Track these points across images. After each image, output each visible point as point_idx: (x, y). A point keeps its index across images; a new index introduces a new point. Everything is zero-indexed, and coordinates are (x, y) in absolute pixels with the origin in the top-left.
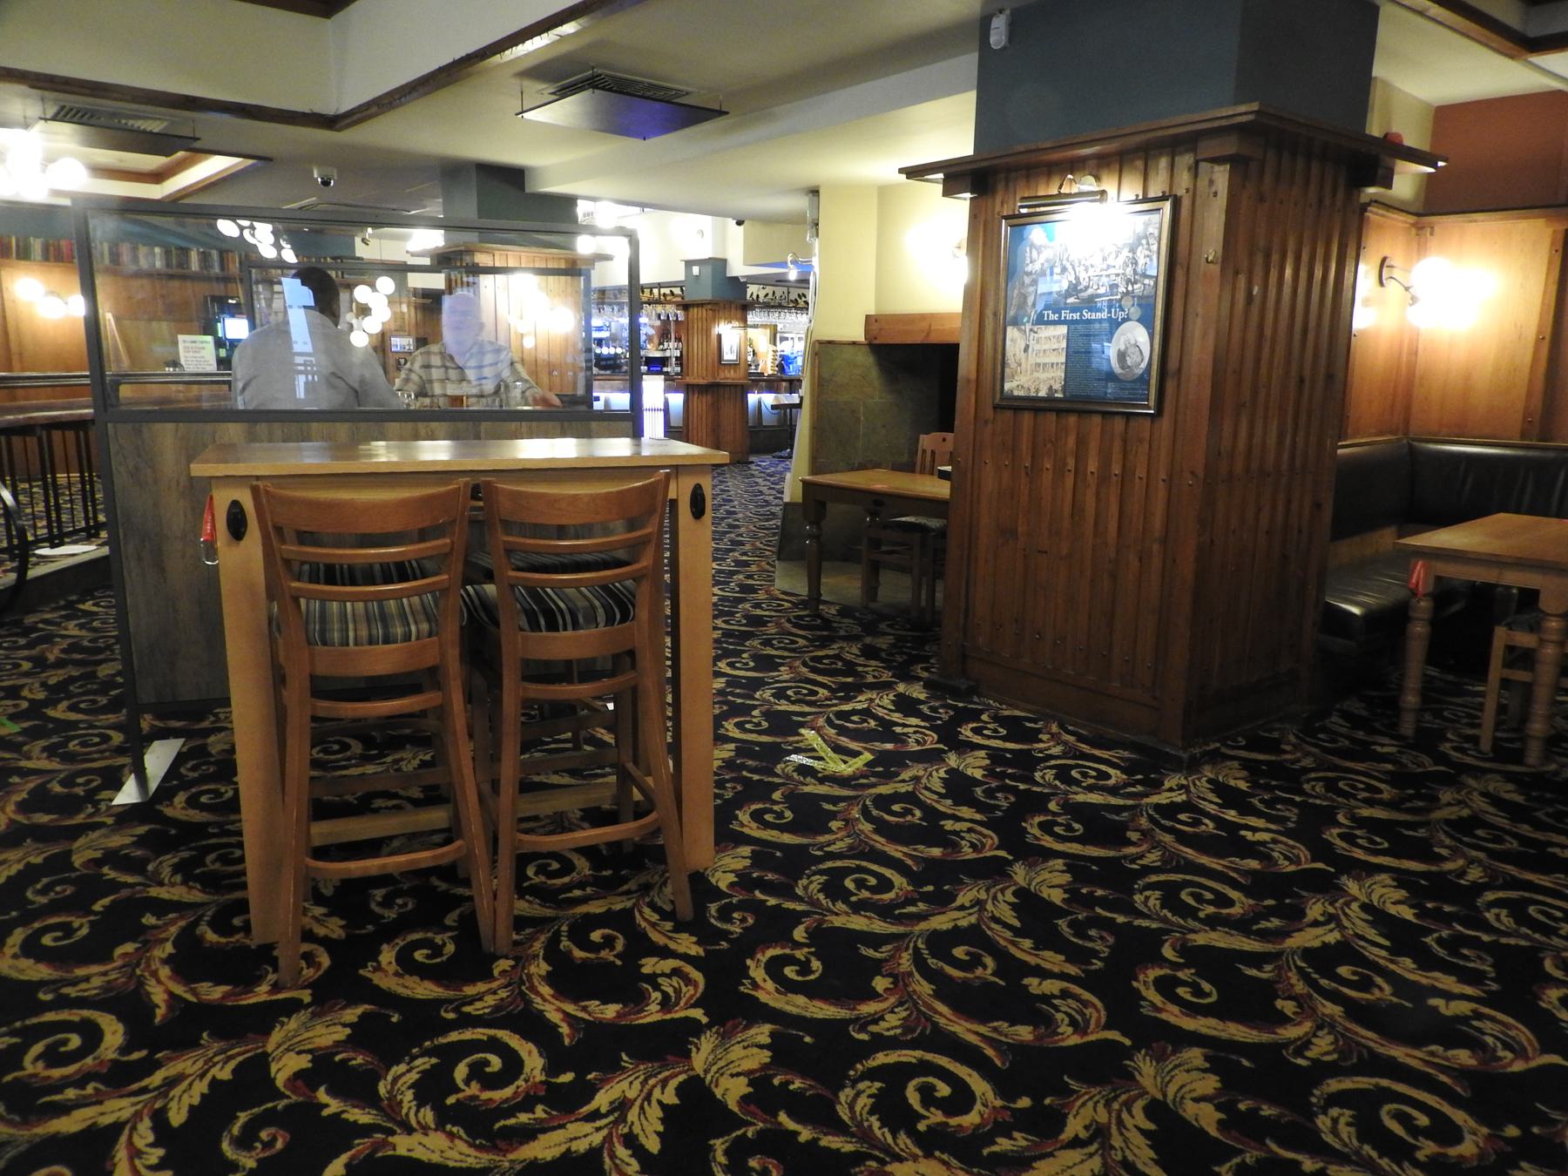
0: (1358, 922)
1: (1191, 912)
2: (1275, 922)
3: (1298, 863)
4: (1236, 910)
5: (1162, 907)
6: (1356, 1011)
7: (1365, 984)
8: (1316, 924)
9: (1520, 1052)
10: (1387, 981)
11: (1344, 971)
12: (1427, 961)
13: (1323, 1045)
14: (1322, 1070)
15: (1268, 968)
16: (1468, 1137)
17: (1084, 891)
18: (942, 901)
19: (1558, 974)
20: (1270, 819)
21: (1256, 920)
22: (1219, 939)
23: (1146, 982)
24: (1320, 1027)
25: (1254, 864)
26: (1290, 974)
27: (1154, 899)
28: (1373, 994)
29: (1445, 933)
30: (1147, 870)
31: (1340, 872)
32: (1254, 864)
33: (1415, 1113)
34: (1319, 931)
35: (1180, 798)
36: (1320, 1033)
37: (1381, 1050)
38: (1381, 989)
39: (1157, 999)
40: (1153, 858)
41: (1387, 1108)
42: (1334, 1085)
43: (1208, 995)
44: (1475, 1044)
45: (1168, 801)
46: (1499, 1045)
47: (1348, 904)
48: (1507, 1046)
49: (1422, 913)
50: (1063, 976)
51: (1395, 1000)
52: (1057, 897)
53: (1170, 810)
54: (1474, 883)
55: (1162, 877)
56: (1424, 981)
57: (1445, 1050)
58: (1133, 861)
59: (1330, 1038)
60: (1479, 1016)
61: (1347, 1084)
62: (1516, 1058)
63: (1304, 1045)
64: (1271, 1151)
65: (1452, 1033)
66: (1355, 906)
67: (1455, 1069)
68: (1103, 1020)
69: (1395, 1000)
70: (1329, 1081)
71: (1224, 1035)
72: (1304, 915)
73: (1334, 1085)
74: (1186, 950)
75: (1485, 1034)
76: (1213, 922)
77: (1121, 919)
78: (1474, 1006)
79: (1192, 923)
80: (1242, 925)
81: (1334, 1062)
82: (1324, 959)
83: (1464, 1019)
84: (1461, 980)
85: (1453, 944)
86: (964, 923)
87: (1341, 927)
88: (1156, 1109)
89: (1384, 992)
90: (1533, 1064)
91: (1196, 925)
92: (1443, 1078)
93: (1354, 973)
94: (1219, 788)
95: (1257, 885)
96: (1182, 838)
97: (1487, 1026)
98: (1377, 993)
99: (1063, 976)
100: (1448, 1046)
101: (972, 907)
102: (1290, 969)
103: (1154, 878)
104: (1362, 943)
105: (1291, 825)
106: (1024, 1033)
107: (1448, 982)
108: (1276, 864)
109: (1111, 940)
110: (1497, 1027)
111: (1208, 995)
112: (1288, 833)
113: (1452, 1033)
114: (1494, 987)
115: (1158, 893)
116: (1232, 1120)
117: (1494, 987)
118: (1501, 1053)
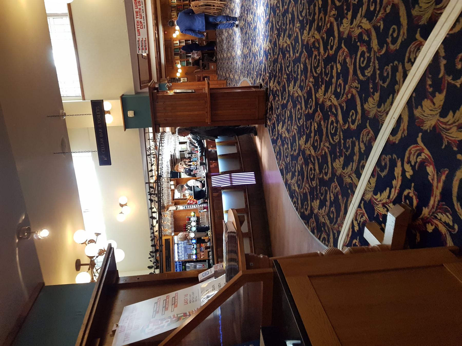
0: (308, 145)
1: (314, 175)
2: (312, 159)
3: (302, 158)
4: (312, 166)
5: (314, 180)
6: (321, 141)
9: (319, 114)
10: (315, 137)
11: (316, 144)
12: (311, 132)
13: (327, 144)
14: (330, 144)
16: (332, 119)
17: (316, 197)
18: (324, 224)
19: (307, 111)
20: (295, 166)
21: (312, 162)
22: (317, 168)
23: (326, 178)
25: (304, 166)
27: (313, 182)
29: (306, 130)
30: (310, 186)
31: (301, 150)
32: (304, 166)
33: (331, 128)
34: (311, 151)
35: (296, 185)
39: (328, 175)
40: (307, 186)
41: (332, 132)
42: (332, 141)
43: (325, 166)
45: (297, 187)
47: (306, 147)
49: (304, 134)
50: (330, 194)
52: (318, 201)
53: (299, 186)
54: (297, 127)
55: (310, 182)
56: (313, 131)
58: (309, 189)
61: (331, 139)
63: (328, 148)
64: (343, 148)
66: (306, 146)
68: (334, 183)
71: (330, 161)
72: (310, 154)
73: (332, 141)
74: (320, 173)
76: (315, 170)
77: (318, 187)
79: (316, 174)
80: (314, 164)
82: (315, 148)
84: (312, 125)
85: (307, 128)
86: (327, 218)
87: (310, 148)
88: (343, 169)
90: (320, 112)
91: (316, 172)
94: (292, 178)
95: (307, 164)
96: (303, 182)
98: (317, 138)
99: (330, 194)
101: (324, 218)
103: (310, 184)
105: (296, 162)
106: (340, 197)
108: (302, 162)
109: (322, 187)
111: (325, 166)
112: (297, 162)
114: (311, 120)
115: (313, 182)
116: (341, 155)
117: (311, 120)
118: (320, 117)
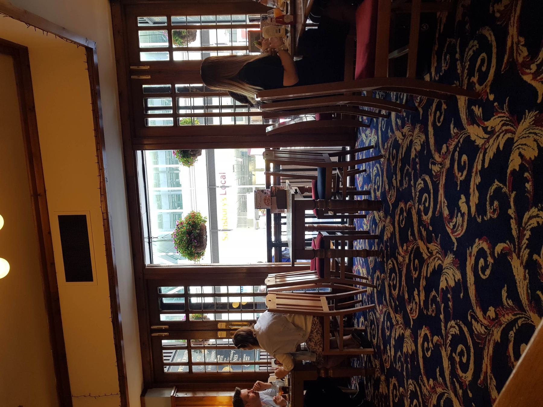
7: (461, 169)
8: (485, 129)
15: (456, 131)
24: (441, 164)
26: (456, 140)
28: (458, 174)
36: (439, 165)
37: (440, 186)
38: (461, 176)
44: (452, 215)
46: (454, 223)
48: (454, 226)
51: (459, 183)
57: (446, 206)
59: (439, 169)
60: (463, 215)
62: (451, 229)
65: (453, 207)
67: (442, 210)
69: (459, 183)
70: (428, 176)
75: (456, 218)
78: (466, 212)
81: (433, 174)
83: (459, 210)
89: (461, 177)
92: (438, 207)
93: (465, 162)
97: (460, 219)
100: (448, 206)
102: (457, 139)
104: (481, 155)
107: (474, 199)
110: (461, 222)
113: (453, 207)
